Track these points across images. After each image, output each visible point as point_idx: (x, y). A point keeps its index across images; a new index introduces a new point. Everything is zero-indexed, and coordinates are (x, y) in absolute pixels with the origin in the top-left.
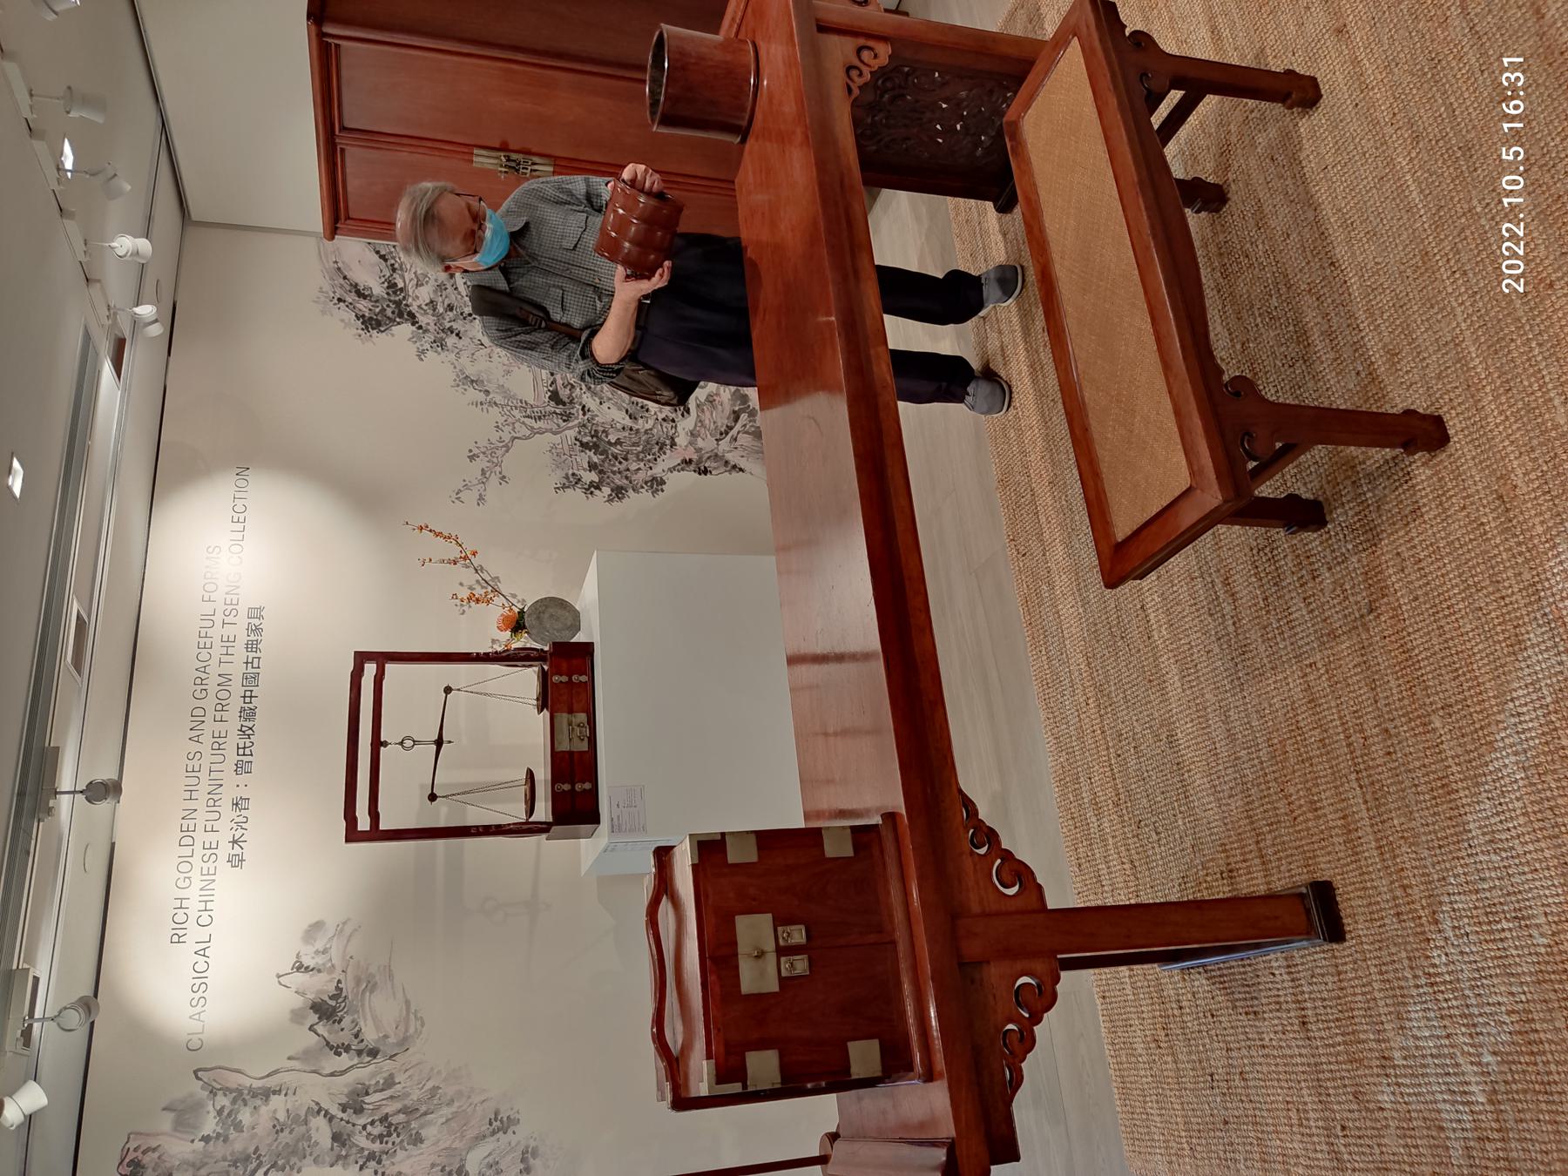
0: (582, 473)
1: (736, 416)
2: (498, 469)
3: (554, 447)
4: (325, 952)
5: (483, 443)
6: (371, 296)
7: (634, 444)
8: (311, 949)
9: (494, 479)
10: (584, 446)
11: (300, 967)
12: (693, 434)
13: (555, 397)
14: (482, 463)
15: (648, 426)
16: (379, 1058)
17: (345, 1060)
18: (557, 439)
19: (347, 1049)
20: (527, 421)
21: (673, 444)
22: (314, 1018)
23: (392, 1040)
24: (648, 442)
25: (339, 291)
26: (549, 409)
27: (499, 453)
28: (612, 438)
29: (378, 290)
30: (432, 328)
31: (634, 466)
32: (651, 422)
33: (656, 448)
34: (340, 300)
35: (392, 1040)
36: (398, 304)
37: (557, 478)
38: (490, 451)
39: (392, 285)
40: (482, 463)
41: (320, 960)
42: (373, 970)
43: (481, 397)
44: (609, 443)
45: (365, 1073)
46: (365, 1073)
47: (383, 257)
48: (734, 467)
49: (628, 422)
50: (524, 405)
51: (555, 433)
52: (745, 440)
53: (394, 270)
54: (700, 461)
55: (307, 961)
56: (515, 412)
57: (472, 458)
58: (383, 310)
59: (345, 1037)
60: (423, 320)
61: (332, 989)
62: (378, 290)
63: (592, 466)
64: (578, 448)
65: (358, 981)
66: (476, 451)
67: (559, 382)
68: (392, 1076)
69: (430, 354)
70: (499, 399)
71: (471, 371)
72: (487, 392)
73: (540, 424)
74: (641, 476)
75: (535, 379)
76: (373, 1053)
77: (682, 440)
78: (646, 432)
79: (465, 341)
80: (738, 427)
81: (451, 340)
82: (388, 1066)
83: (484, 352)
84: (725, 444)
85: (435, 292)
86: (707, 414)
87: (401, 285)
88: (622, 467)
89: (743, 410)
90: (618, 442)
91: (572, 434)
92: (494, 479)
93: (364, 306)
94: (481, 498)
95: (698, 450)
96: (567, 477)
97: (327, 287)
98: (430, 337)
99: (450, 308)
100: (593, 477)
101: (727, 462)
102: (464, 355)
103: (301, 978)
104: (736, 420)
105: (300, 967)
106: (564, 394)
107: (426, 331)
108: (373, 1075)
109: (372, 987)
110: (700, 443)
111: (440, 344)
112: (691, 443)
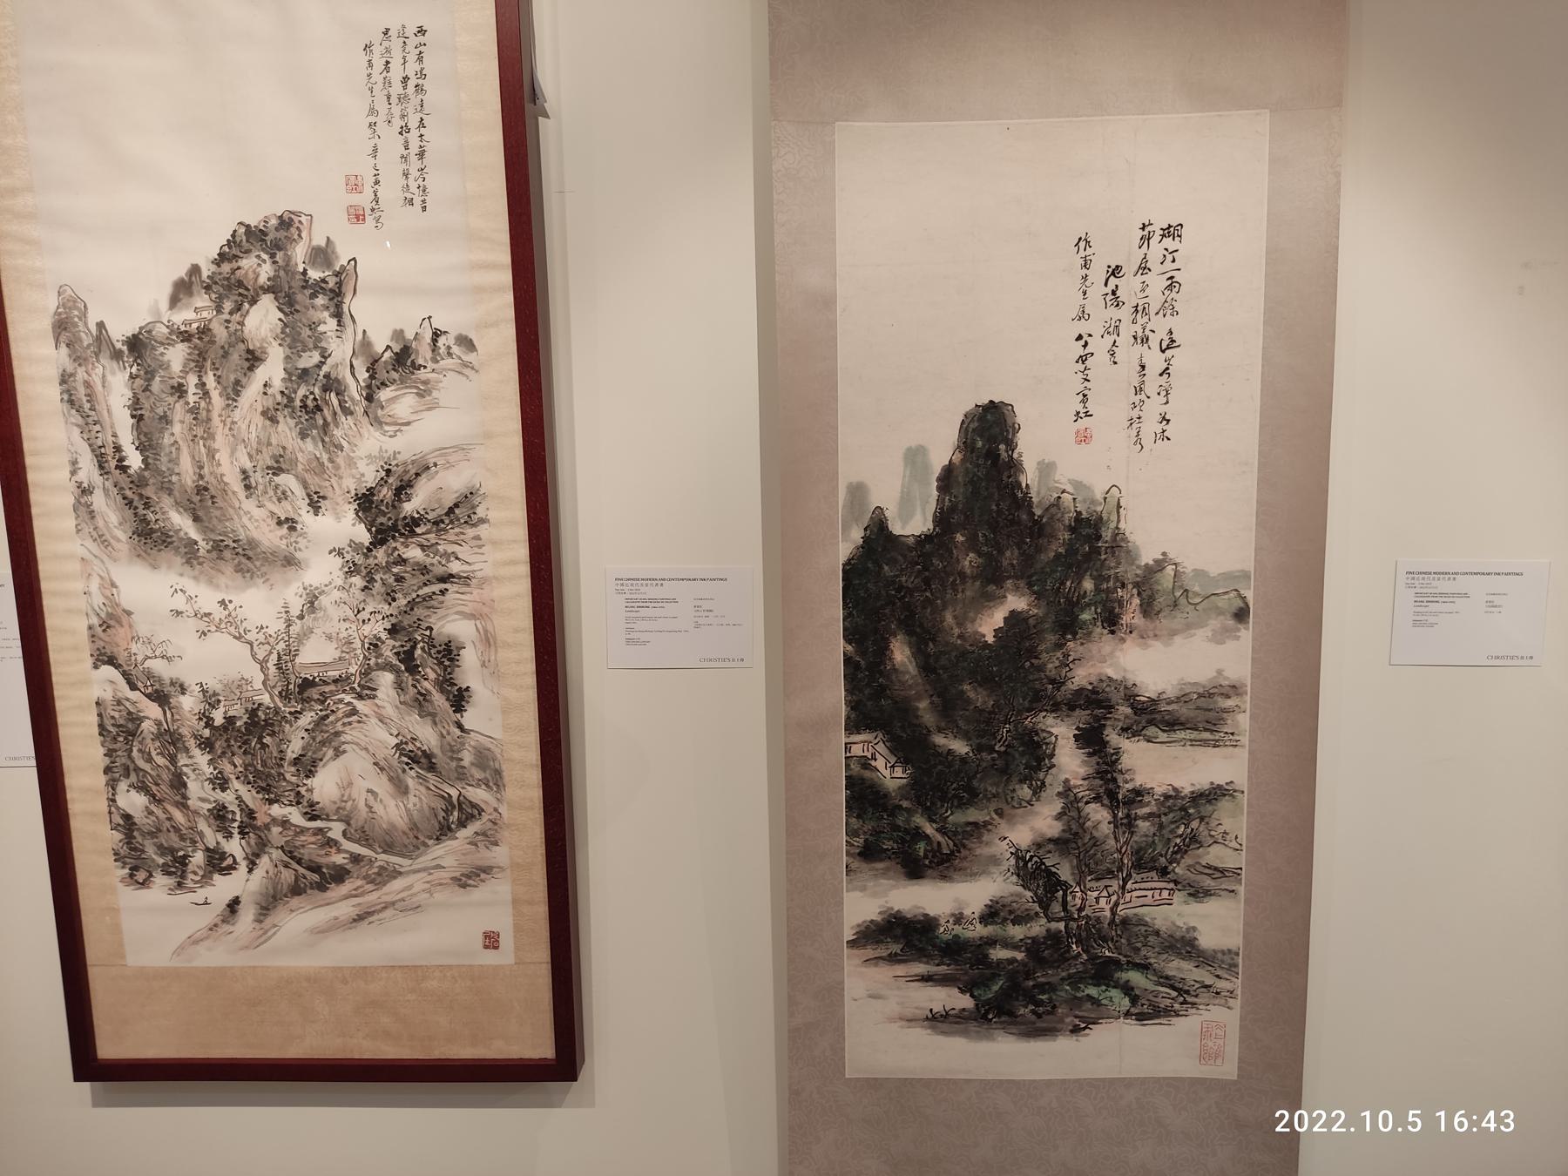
0: (222, 710)
1: (315, 868)
2: (213, 628)
3: (248, 682)
4: (450, 354)
5: (241, 614)
6: (400, 501)
7: (264, 764)
8: (451, 342)
9: (202, 626)
10: (253, 713)
11: (436, 334)
12: (285, 823)
13: (307, 684)
14: (219, 613)
15: (288, 776)
16: (364, 403)
17: (363, 375)
18: (258, 685)
19: (372, 377)
20: (274, 657)
21: (271, 802)
22: (397, 348)
23: (380, 412)
24: (269, 775)
25: (401, 469)
26: (293, 678)
27: (232, 629)
28: (268, 740)
29: (409, 508)
30: (371, 561)
31: (238, 761)
32: (294, 779)
33: (264, 785)
34: (388, 472)
35: (380, 412)
36: (395, 528)
37: (213, 685)
38: (231, 620)
39: (415, 522)
40: (219, 613)
41: (442, 350)
42: (435, 394)
43: (295, 612)
44: (260, 738)
45: (354, 391)
46: (354, 391)
47: (451, 511)
48: (254, 863)
49: (290, 755)
50: (292, 653)
51: (264, 683)
52: (287, 876)
53: (436, 523)
54: (255, 828)
55: (442, 341)
56: (282, 645)
57: (222, 603)
58: (384, 514)
59: (382, 375)
60: (380, 554)
61: (420, 361)
62: (409, 508)
63: (230, 720)
64: (250, 706)
65: (425, 383)
66: (231, 607)
67: (327, 689)
68: (351, 413)
69: (339, 561)
70: (296, 628)
71: (324, 601)
72: (301, 617)
73: (272, 670)
74: (228, 768)
75: (326, 664)
76: (369, 398)
77: (276, 810)
78: (280, 774)
79: (360, 596)
80: (301, 870)
81: (358, 581)
82: (359, 410)
83: (350, 614)
84: (277, 854)
85: (418, 564)
86: (313, 839)
87: (418, 530)
88: (235, 749)
89: (322, 875)
90: (264, 746)
91: (266, 699)
92: (202, 626)
93: (386, 493)
94: (179, 613)
95: (267, 827)
96: (215, 694)
97: (401, 458)
98: (359, 559)
99: (399, 579)
100: (219, 719)
101: (258, 856)
102: (344, 595)
103: (428, 336)
104: (309, 868)
105: (436, 334)
106: (314, 693)
107: (366, 556)
108: (352, 399)
109: (420, 395)
110: (276, 830)
111: (353, 569)
112: (274, 819)
